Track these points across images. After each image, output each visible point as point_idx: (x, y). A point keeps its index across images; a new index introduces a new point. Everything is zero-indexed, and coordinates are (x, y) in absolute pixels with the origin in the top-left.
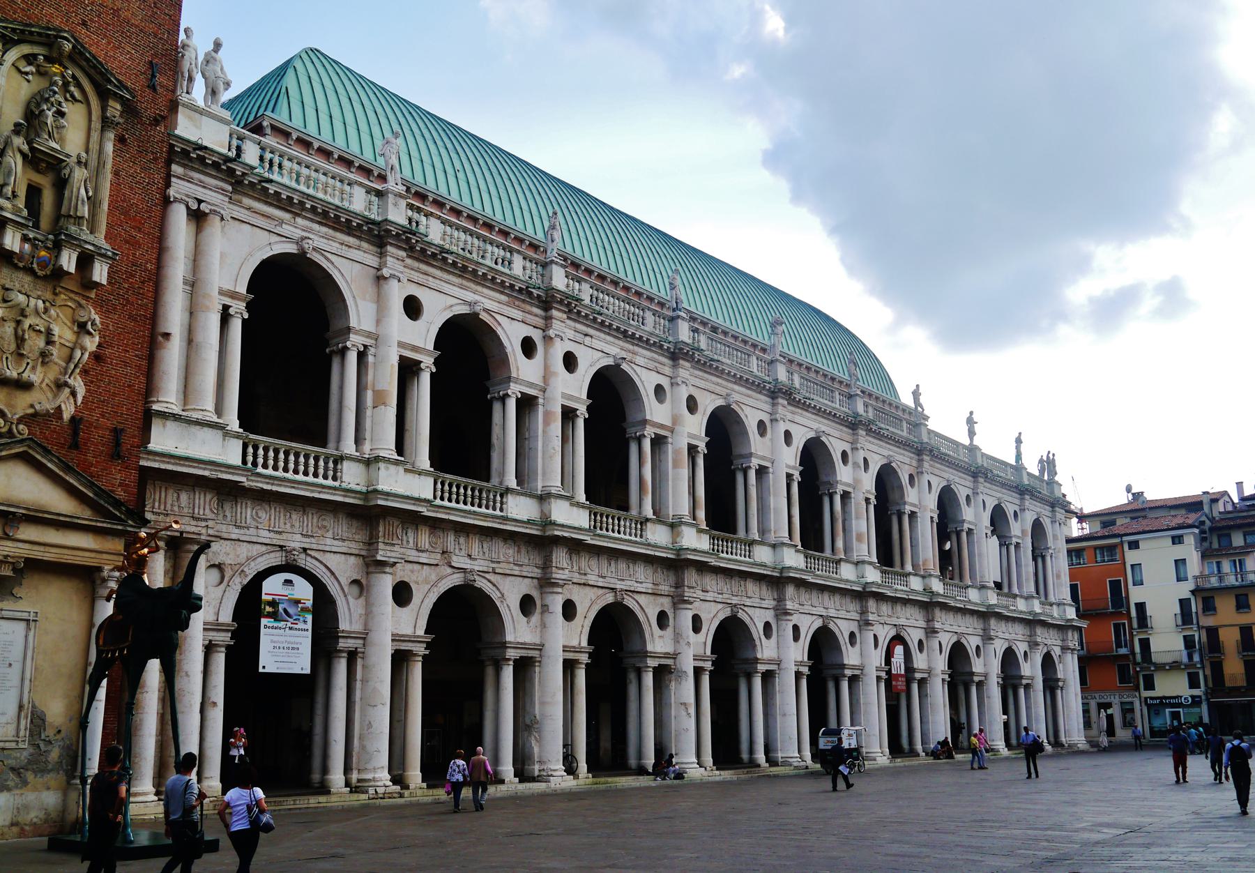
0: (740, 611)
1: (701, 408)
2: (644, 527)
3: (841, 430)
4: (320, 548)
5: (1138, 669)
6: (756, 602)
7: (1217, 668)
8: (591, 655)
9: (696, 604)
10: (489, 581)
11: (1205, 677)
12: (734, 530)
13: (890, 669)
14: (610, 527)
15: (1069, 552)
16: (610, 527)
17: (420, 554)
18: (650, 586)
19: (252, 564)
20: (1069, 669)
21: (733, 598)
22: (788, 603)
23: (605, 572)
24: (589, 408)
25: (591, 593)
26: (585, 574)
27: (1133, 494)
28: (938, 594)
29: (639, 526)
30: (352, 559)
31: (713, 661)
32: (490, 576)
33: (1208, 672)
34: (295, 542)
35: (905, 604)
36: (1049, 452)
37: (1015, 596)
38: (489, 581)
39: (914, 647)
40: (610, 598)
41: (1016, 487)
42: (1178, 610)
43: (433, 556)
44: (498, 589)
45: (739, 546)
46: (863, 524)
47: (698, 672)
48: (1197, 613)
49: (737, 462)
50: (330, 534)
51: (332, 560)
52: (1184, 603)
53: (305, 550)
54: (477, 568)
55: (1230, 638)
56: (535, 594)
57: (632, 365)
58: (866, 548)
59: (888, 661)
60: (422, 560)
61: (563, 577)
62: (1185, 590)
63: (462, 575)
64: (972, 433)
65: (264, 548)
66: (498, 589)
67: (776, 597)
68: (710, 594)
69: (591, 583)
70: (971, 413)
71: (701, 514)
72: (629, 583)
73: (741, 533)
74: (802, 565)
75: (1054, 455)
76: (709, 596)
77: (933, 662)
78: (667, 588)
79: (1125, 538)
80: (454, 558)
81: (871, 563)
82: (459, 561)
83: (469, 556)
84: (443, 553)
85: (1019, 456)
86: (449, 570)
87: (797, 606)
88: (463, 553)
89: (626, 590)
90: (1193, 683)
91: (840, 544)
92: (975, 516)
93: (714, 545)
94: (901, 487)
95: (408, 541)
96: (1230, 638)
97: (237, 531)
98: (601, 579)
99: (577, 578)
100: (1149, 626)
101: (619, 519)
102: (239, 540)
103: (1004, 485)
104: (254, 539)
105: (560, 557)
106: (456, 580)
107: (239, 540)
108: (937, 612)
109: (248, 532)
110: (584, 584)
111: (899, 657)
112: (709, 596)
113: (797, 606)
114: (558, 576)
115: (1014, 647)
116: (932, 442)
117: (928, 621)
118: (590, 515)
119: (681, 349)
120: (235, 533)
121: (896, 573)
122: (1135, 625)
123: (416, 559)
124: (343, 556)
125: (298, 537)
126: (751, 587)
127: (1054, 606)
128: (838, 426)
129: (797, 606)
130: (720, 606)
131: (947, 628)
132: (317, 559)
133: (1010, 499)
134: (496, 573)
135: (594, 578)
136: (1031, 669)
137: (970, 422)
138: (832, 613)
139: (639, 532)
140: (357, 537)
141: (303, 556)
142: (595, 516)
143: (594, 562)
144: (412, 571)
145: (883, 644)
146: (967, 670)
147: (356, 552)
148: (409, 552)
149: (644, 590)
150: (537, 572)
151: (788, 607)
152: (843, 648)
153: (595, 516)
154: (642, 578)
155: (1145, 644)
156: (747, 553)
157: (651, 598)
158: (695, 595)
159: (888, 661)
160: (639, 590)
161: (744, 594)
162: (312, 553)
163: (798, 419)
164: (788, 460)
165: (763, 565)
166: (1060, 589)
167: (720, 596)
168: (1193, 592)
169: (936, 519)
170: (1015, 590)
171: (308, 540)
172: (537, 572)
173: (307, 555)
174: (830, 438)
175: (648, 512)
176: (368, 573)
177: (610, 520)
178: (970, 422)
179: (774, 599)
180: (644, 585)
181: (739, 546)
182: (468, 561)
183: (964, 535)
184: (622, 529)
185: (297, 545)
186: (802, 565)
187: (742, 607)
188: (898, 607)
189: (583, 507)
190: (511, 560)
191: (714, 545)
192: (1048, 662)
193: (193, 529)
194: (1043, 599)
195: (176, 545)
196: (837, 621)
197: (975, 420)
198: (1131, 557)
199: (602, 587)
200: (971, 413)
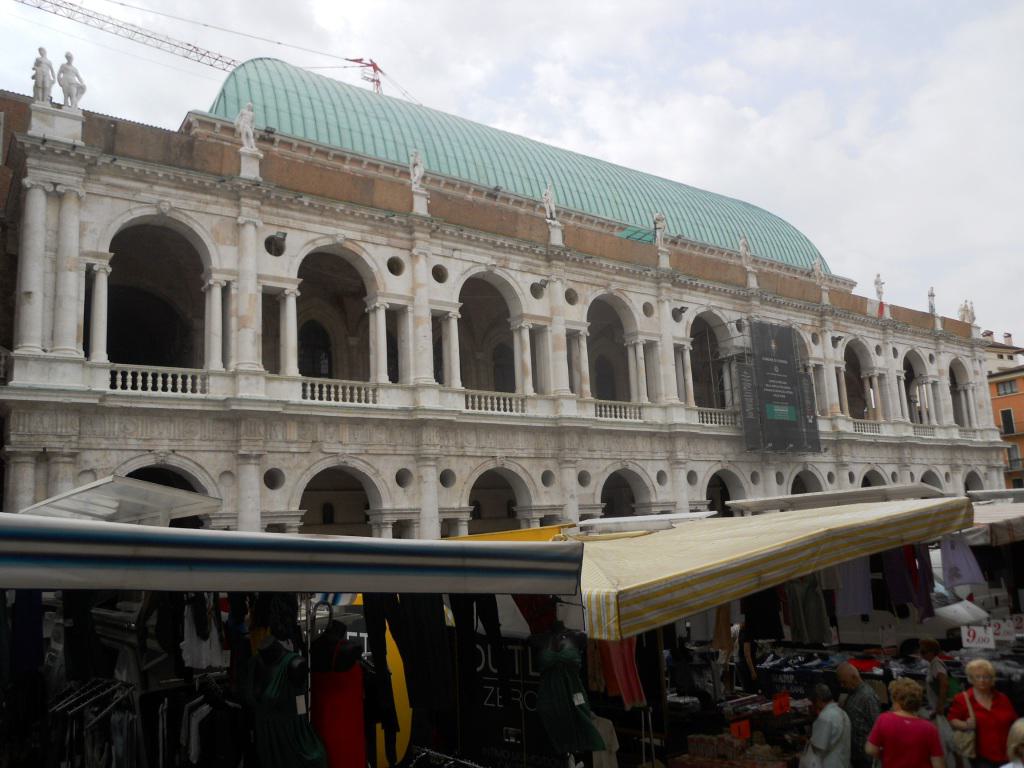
0: (630, 464)
4: (189, 448)
6: (648, 455)
10: (364, 461)
17: (290, 445)
18: (533, 451)
19: (123, 467)
22: (679, 453)
23: (483, 443)
25: (471, 463)
26: (462, 448)
28: (845, 433)
30: (222, 456)
32: (365, 458)
34: (164, 446)
37: (933, 428)
38: (364, 461)
40: (491, 465)
43: (303, 445)
44: (372, 467)
50: (197, 437)
51: (201, 458)
53: (173, 451)
54: (348, 452)
56: (410, 467)
60: (292, 450)
61: (435, 452)
63: (335, 458)
65: (133, 454)
66: (372, 467)
67: (668, 448)
69: (468, 454)
72: (510, 451)
76: (597, 455)
80: (326, 446)
82: (331, 447)
83: (341, 442)
84: (313, 442)
86: (321, 456)
88: (334, 440)
95: (277, 436)
97: (106, 442)
98: (479, 451)
102: (108, 449)
104: (124, 447)
106: (329, 463)
107: (108, 449)
108: (846, 448)
109: (116, 442)
113: (691, 455)
114: (430, 452)
117: (837, 456)
119: (552, 252)
120: (104, 444)
123: (286, 450)
124: (212, 455)
125: (166, 442)
127: (978, 433)
131: (859, 460)
132: (185, 458)
134: (370, 454)
140: (225, 437)
141: (172, 456)
143: (472, 438)
144: (283, 460)
147: (226, 449)
148: (277, 444)
149: (525, 455)
150: (412, 450)
151: (680, 457)
154: (521, 446)
157: (536, 462)
160: (520, 455)
161: (634, 449)
162: (181, 453)
171: (175, 443)
172: (412, 450)
173: (177, 455)
176: (238, 465)
179: (667, 452)
180: (526, 451)
182: (341, 446)
185: (166, 448)
190: (384, 442)
193: (57, 445)
195: (44, 457)
199: (482, 457)
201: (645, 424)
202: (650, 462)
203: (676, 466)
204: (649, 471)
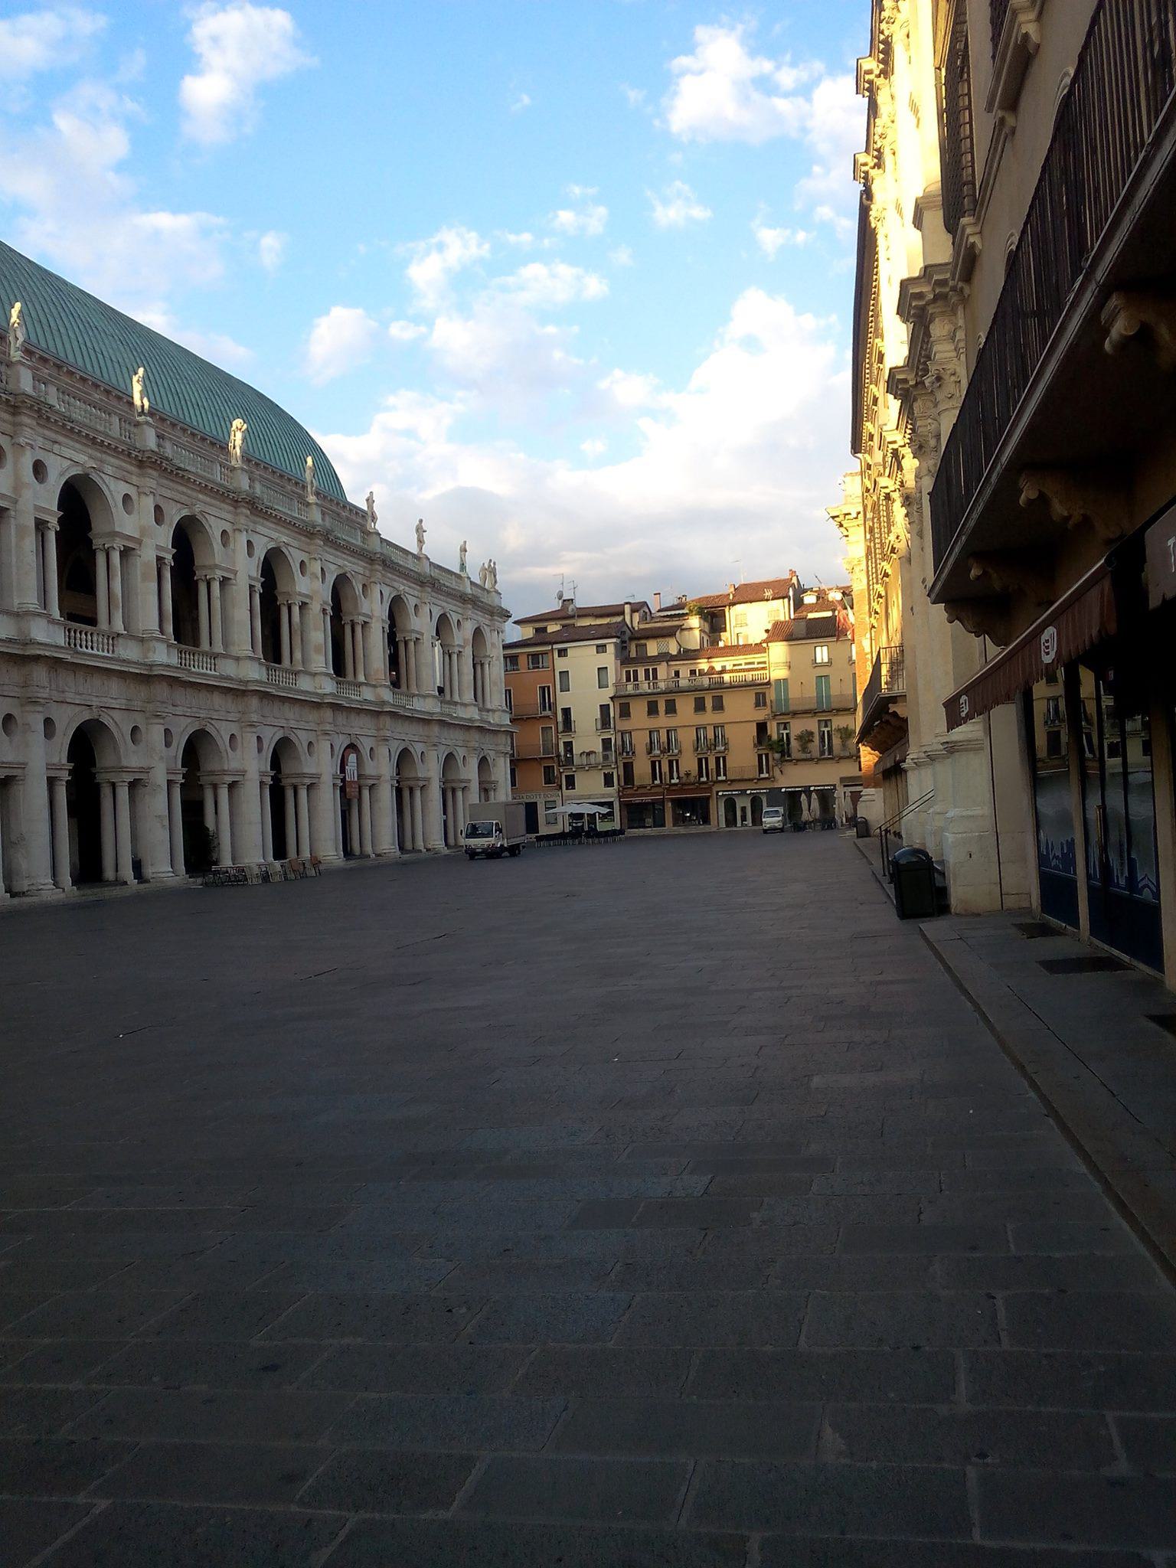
1: (167, 518)
2: (115, 642)
3: (299, 540)
5: (561, 771)
7: (628, 768)
8: (71, 772)
9: (167, 719)
11: (618, 776)
12: (196, 643)
13: (345, 777)
14: (84, 643)
15: (505, 657)
16: (84, 643)
18: (124, 701)
20: (501, 771)
21: (201, 711)
24: (60, 521)
25: (70, 711)
26: (63, 692)
27: (564, 601)
29: (111, 641)
31: (184, 774)
33: (621, 773)
35: (359, 714)
36: (490, 561)
37: (456, 704)
39: (365, 752)
40: (86, 716)
41: (461, 597)
42: (599, 716)
45: (205, 660)
46: (319, 635)
47: (170, 783)
48: (614, 717)
49: (199, 574)
52: (605, 709)
55: (640, 741)
57: (101, 474)
58: (321, 661)
59: (343, 770)
61: (45, 696)
62: (605, 696)
64: (421, 541)
68: (180, 708)
69: (68, 700)
70: (421, 521)
71: (169, 628)
73: (205, 645)
74: (264, 678)
75: (494, 563)
76: (179, 710)
77: (383, 768)
78: (140, 703)
79: (555, 646)
81: (327, 675)
85: (463, 567)
87: (261, 719)
89: (101, 707)
90: (608, 781)
91: (298, 655)
92: (421, 623)
93: (181, 659)
94: (355, 598)
96: (640, 741)
98: (78, 697)
99: (56, 696)
100: (573, 730)
101: (91, 634)
103: (448, 594)
105: (40, 675)
110: (62, 702)
111: (353, 764)
112: (179, 710)
115: (455, 753)
116: (385, 552)
118: (65, 632)
121: (349, 683)
122: (561, 728)
126: (217, 700)
128: (297, 536)
129: (261, 719)
130: (189, 720)
133: (454, 608)
135: (71, 695)
136: (470, 772)
137: (420, 530)
138: (293, 724)
139: (111, 648)
142: (69, 632)
145: (339, 752)
146: (412, 775)
152: (303, 758)
153: (69, 632)
154: (114, 693)
155: (569, 746)
156: (213, 667)
158: (167, 710)
159: (343, 770)
163: (259, 528)
164: (247, 570)
165: (228, 678)
166: (496, 699)
167: (189, 710)
168: (612, 698)
169: (387, 630)
170: (456, 698)
174: (289, 548)
175: (119, 626)
177: (84, 636)
178: (420, 530)
180: (118, 701)
181: (205, 660)
183: (411, 645)
184: (95, 645)
186: (264, 678)
187: (210, 721)
188: (353, 716)
189: (57, 624)
191: (181, 659)
192: (483, 762)
194: (481, 706)
196: (298, 732)
197: (425, 528)
198: (561, 664)
200: (421, 521)
201: (222, 677)
202: (224, 723)
203: (248, 729)
204: (222, 733)
